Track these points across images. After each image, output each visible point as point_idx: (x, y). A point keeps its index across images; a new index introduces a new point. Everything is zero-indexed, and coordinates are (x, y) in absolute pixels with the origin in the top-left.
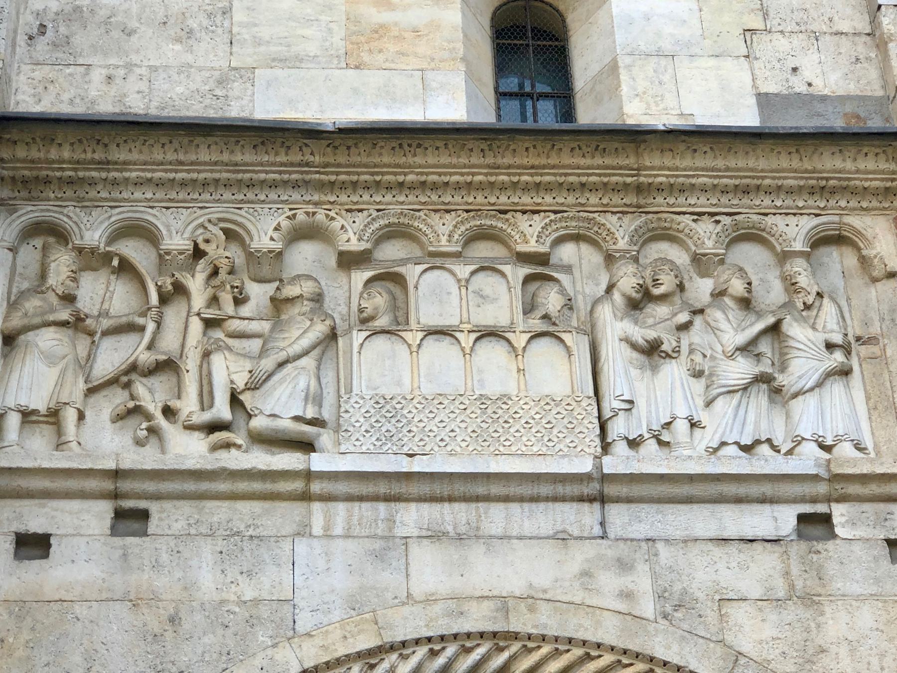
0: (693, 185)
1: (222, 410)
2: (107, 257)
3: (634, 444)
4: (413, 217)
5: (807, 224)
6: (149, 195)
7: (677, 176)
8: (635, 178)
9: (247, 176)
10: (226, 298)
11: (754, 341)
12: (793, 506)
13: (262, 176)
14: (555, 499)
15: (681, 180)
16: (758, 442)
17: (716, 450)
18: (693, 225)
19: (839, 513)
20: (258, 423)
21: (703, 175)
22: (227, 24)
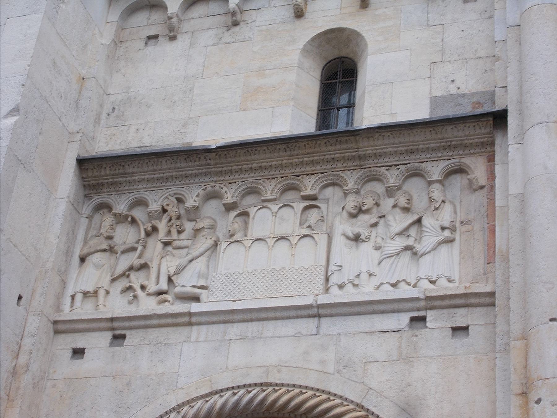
0: (385, 153)
1: (164, 285)
2: (127, 216)
3: (341, 287)
4: (257, 183)
5: (443, 165)
6: (145, 186)
7: (377, 149)
8: (357, 153)
9: (184, 173)
10: (174, 231)
11: (407, 228)
12: (409, 313)
13: (190, 172)
14: (297, 317)
15: (379, 151)
16: (398, 282)
17: (379, 287)
18: (386, 172)
19: (430, 315)
20: (178, 289)
21: (389, 147)
22: (191, 96)
